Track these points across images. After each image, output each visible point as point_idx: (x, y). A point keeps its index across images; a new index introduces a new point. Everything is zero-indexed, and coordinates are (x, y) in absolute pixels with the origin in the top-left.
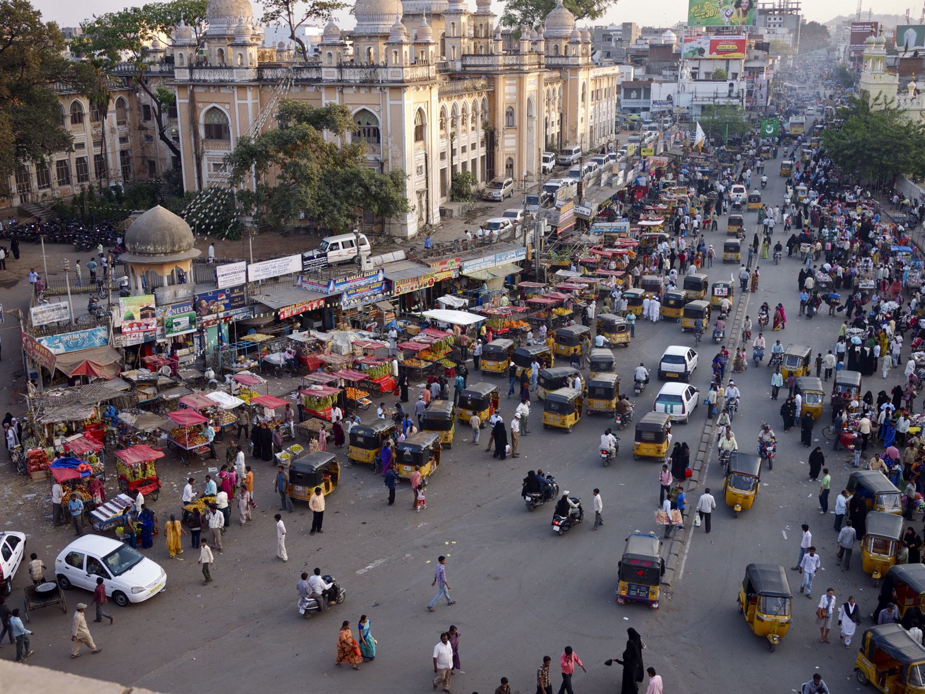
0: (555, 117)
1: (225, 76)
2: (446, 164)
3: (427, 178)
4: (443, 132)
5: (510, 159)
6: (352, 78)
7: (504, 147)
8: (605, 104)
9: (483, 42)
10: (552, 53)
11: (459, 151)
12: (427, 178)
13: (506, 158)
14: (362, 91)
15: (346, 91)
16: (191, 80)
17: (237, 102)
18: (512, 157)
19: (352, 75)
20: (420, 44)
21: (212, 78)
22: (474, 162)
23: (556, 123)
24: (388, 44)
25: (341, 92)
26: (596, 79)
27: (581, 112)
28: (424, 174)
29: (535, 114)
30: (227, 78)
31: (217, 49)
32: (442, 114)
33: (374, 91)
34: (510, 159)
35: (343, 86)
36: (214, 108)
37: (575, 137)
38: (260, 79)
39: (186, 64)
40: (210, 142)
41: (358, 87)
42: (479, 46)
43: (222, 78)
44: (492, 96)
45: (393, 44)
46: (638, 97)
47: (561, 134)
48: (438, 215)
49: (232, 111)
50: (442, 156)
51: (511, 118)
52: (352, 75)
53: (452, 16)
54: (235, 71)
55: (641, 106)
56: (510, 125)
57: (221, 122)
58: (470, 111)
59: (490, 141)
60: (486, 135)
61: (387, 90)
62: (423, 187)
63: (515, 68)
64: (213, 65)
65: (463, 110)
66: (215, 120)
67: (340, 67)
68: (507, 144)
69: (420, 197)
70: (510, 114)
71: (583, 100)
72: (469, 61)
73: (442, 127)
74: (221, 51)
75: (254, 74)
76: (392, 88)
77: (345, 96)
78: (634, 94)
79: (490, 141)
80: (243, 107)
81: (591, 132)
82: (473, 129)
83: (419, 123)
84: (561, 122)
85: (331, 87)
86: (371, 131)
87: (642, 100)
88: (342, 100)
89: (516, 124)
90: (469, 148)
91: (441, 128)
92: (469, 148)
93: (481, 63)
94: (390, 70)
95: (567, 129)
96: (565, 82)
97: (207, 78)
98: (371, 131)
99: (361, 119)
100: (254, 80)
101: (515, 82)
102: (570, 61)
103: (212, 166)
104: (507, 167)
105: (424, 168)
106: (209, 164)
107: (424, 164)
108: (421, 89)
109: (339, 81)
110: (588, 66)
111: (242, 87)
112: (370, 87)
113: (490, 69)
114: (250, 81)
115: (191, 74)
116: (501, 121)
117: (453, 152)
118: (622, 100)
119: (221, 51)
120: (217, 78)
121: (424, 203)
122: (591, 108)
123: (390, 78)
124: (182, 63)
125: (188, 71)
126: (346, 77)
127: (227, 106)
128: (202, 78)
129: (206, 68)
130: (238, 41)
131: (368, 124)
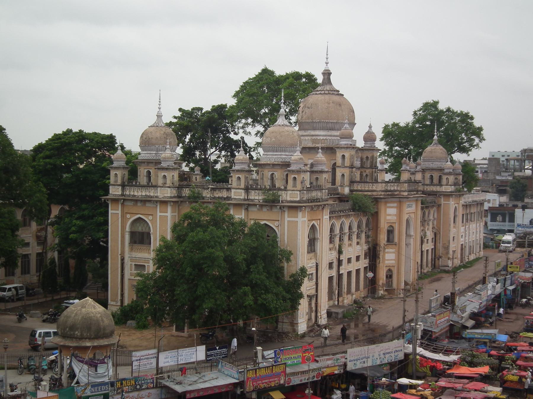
0: (430, 235)
1: (151, 193)
2: (334, 273)
3: (317, 284)
4: (332, 246)
5: (390, 270)
6: (257, 198)
7: (384, 259)
8: (474, 225)
9: (368, 171)
10: (428, 182)
11: (345, 262)
12: (317, 284)
14: (265, 209)
15: (251, 209)
16: (122, 195)
17: (159, 214)
18: (392, 268)
19: (256, 196)
20: (316, 172)
21: (140, 194)
22: (358, 271)
23: (430, 241)
24: (289, 171)
25: (247, 209)
26: (466, 206)
27: (453, 231)
28: (315, 280)
29: (412, 233)
30: (152, 194)
32: (332, 230)
33: (275, 210)
34: (390, 270)
35: (249, 205)
36: (140, 218)
37: (448, 253)
38: (179, 197)
39: (119, 182)
41: (261, 206)
42: (364, 175)
43: (148, 194)
44: (376, 216)
45: (293, 171)
46: (504, 221)
47: (434, 250)
48: (325, 316)
49: (154, 221)
50: (331, 265)
52: (256, 196)
53: (343, 150)
54: (159, 189)
55: (506, 228)
56: (390, 240)
57: (144, 230)
58: (355, 229)
59: (373, 254)
60: (369, 249)
61: (286, 209)
62: (313, 292)
63: (396, 193)
64: (142, 184)
65: (350, 228)
66: (140, 228)
67: (247, 189)
68: (388, 257)
69: (310, 301)
70: (390, 232)
71: (454, 222)
72: (356, 187)
73: (331, 241)
74: (149, 173)
75: (175, 192)
76: (290, 208)
77: (250, 213)
78: (499, 218)
79: (373, 254)
80: (164, 219)
81: (462, 249)
82: (358, 243)
83: (311, 237)
84: (435, 240)
85: (238, 206)
87: (507, 223)
88: (247, 215)
89: (396, 240)
90: (354, 260)
91: (331, 242)
92: (354, 260)
93: (367, 189)
94: (289, 192)
95: (440, 246)
96: (439, 206)
97: (136, 194)
100: (174, 197)
101: (395, 205)
102: (444, 189)
103: (133, 266)
104: (387, 277)
105: (314, 275)
107: (314, 272)
108: (315, 209)
109: (245, 200)
110: (458, 194)
111: (164, 203)
112: (271, 207)
113: (374, 193)
114: (171, 197)
115: (123, 190)
116: (383, 238)
117: (340, 263)
118: (489, 223)
119: (149, 173)
120: (144, 194)
121: (313, 305)
122: (462, 229)
123: (289, 199)
124: (116, 181)
125: (120, 188)
126: (251, 197)
127: (151, 217)
128: (132, 193)
129: (136, 186)
130: (164, 165)
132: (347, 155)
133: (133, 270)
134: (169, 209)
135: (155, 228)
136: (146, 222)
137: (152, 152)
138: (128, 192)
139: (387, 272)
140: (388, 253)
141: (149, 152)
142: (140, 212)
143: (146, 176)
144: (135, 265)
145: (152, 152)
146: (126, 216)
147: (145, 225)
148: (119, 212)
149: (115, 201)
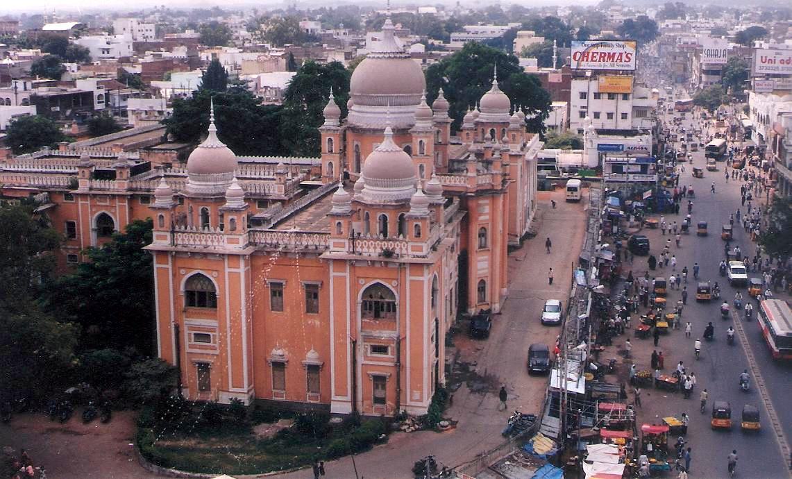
13: (478, 281)
17: (227, 270)
18: (485, 279)
28: (435, 342)
31: (201, 208)
40: (192, 309)
49: (221, 279)
51: (483, 239)
66: (198, 287)
80: (235, 277)
86: (385, 306)
98: (385, 306)
99: (373, 293)
103: (193, 336)
106: (190, 334)
116: (475, 242)
127: (215, 274)
131: (381, 297)
132: (425, 141)
133: (193, 340)
134: (242, 263)
135: (223, 290)
136: (208, 278)
137: (208, 183)
138: (181, 239)
139: (479, 283)
140: (479, 261)
141: (204, 183)
142: (199, 267)
143: (202, 216)
144: (195, 334)
145: (208, 183)
146: (179, 273)
147: (207, 283)
148: (170, 266)
149: (163, 253)
